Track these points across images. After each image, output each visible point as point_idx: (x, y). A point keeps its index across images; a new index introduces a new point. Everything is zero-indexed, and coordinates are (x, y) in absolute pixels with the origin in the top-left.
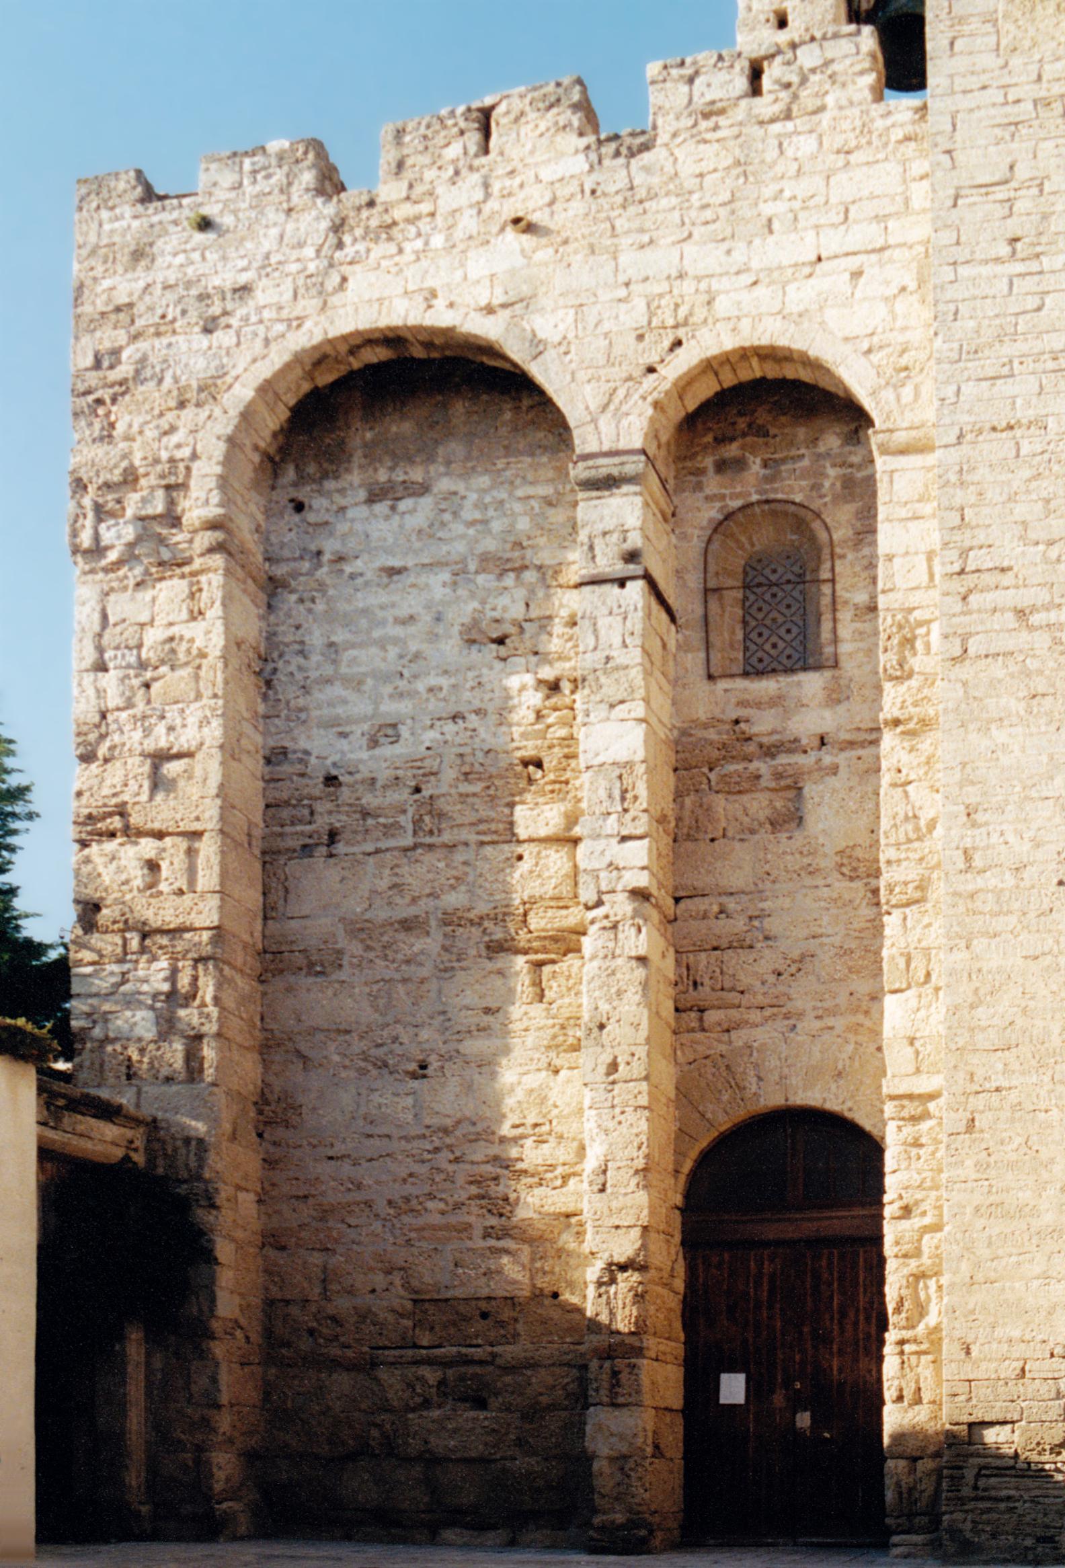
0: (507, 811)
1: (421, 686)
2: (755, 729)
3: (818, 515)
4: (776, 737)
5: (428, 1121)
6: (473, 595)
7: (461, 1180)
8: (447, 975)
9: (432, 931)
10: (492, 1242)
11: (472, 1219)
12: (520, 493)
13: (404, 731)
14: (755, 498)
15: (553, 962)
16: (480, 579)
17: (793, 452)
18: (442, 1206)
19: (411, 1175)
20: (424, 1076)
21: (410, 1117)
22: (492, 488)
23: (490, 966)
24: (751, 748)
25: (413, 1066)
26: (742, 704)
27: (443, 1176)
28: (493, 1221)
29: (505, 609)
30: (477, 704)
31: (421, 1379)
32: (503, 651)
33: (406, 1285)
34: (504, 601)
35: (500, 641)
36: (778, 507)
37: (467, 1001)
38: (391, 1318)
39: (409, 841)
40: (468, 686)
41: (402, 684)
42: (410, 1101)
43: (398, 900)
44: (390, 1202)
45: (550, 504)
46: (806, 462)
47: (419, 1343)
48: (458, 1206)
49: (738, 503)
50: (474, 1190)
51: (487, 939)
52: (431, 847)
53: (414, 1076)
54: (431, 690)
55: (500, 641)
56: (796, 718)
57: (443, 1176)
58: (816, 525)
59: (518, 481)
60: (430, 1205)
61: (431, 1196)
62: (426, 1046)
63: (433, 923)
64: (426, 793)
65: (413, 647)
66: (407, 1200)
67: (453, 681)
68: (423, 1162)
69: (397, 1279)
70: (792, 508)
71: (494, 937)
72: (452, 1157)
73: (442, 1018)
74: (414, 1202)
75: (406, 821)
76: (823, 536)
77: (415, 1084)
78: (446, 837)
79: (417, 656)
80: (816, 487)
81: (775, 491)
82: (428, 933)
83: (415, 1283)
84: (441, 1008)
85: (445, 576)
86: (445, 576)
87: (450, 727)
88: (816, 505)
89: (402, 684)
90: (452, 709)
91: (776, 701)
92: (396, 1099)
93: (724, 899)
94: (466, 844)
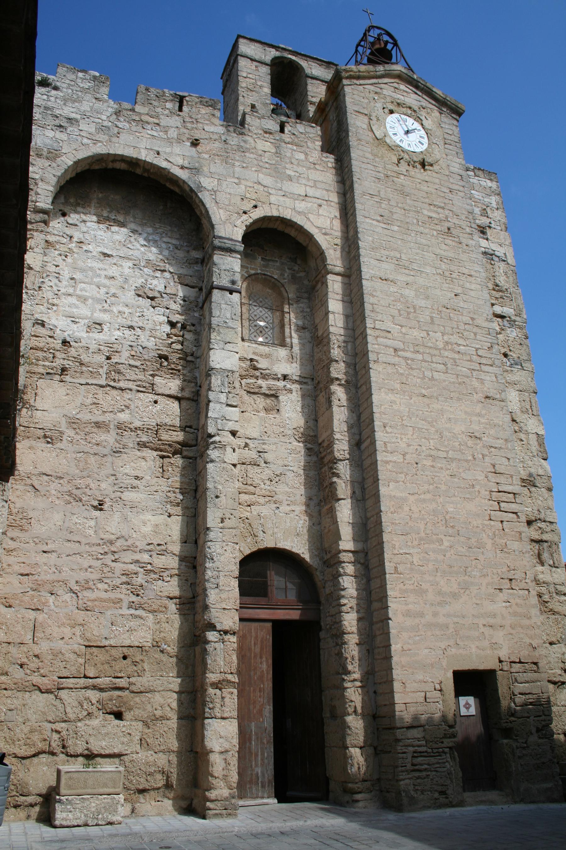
0: (151, 378)
1: (115, 309)
2: (259, 366)
3: (283, 286)
4: (267, 371)
5: (103, 536)
6: (142, 276)
7: (118, 573)
8: (117, 455)
9: (111, 431)
10: (132, 611)
11: (122, 596)
12: (165, 240)
13: (105, 327)
14: (259, 271)
15: (169, 457)
16: (146, 270)
17: (273, 259)
18: (106, 586)
19: (90, 567)
20: (101, 510)
21: (91, 532)
22: (152, 234)
23: (139, 453)
24: (258, 373)
25: (96, 503)
26: (254, 353)
27: (108, 569)
28: (134, 598)
29: (156, 286)
30: (141, 324)
31: (87, 699)
32: (154, 303)
33: (83, 636)
34: (155, 282)
35: (152, 299)
36: (268, 278)
37: (127, 471)
38: (73, 657)
39: (103, 382)
40: (138, 314)
41: (106, 306)
42: (92, 523)
43: (96, 412)
44: (77, 582)
45: (177, 248)
46: (278, 264)
47: (89, 675)
48: (115, 587)
49: (253, 272)
50: (124, 579)
51: (138, 440)
52: (113, 387)
53: (95, 508)
54: (119, 312)
55: (152, 299)
56: (276, 366)
57: (108, 569)
58: (282, 289)
59: (164, 235)
60: (100, 586)
61: (101, 580)
62: (104, 493)
63: (112, 427)
64: (114, 360)
65: (113, 291)
66: (87, 582)
67: (130, 311)
68: (98, 559)
69: (78, 630)
70: (273, 280)
71: (143, 440)
72: (113, 558)
73: (114, 478)
74: (91, 583)
75: (102, 371)
76: (285, 294)
77: (98, 513)
78: (122, 384)
79: (114, 295)
80: (282, 275)
81: (267, 271)
82: (109, 431)
83: (88, 635)
84: (113, 473)
85: (130, 264)
86: (130, 264)
87: (127, 332)
88: (283, 281)
89: (106, 306)
90: (130, 323)
91: (267, 356)
92: (85, 521)
93: (248, 441)
94: (131, 390)
